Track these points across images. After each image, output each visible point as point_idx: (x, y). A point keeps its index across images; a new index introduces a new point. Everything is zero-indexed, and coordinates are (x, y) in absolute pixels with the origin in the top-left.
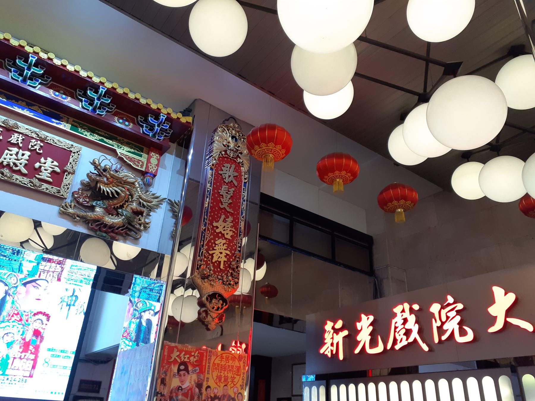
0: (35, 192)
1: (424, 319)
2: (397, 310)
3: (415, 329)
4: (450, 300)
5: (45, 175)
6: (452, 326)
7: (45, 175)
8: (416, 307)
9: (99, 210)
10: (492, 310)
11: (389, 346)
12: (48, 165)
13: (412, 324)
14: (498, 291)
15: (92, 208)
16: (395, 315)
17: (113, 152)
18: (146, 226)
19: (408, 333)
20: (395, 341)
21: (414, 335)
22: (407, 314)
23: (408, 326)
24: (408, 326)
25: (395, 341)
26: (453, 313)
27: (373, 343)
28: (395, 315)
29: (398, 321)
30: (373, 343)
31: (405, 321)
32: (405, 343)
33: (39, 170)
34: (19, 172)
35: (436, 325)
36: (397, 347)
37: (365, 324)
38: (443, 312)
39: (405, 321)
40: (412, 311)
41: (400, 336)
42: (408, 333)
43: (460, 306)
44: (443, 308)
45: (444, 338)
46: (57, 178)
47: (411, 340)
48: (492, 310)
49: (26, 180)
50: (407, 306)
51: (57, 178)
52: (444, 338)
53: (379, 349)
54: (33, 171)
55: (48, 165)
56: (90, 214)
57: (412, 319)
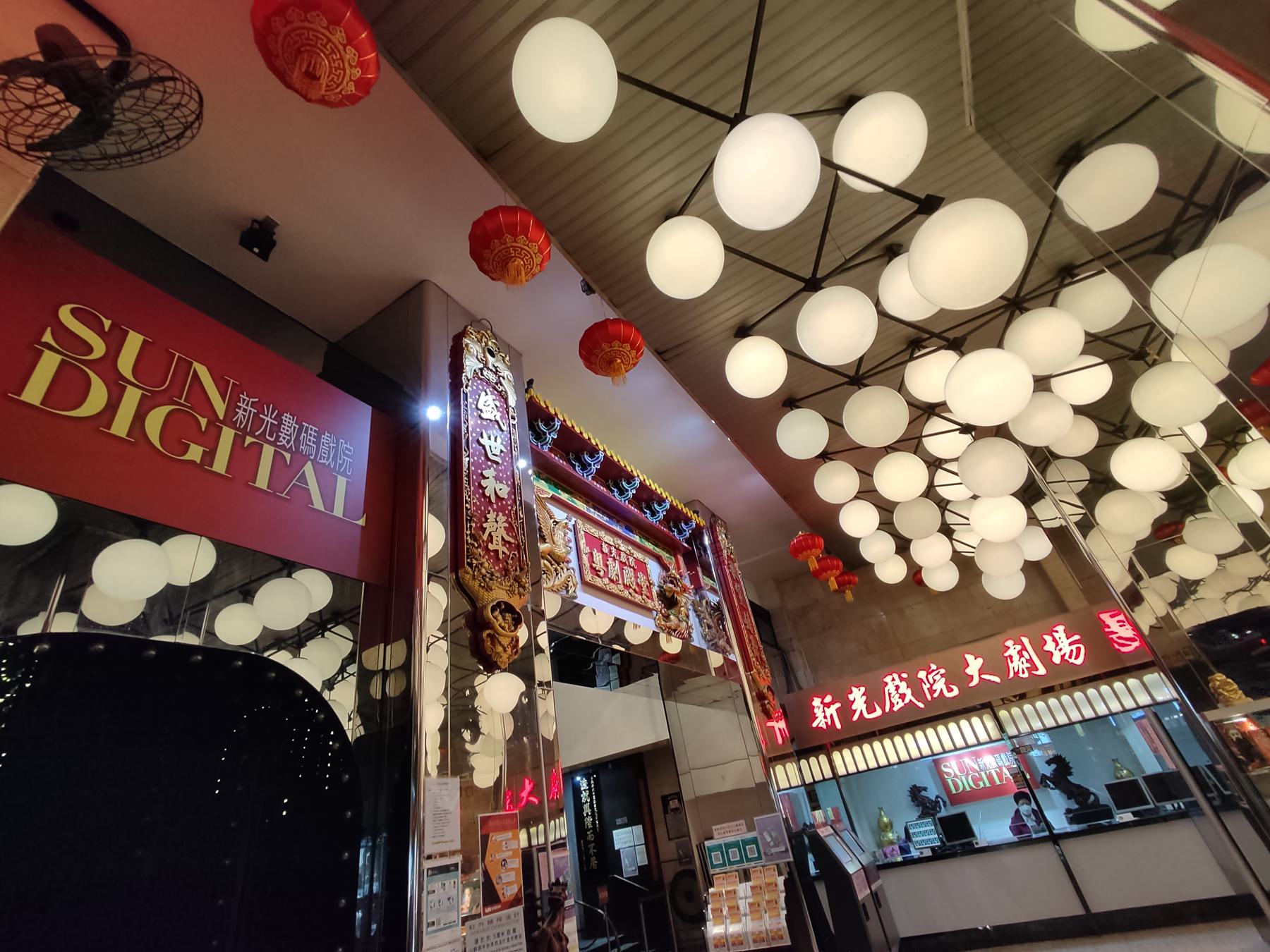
1: (915, 685)
2: (888, 679)
3: (908, 692)
4: (933, 667)
8: (904, 675)
11: (887, 709)
13: (903, 688)
20: (892, 705)
21: (909, 697)
22: (897, 682)
25: (892, 705)
27: (871, 709)
29: (890, 688)
30: (871, 709)
31: (897, 687)
32: (901, 704)
36: (896, 708)
37: (858, 698)
38: (930, 677)
39: (897, 687)
40: (902, 679)
41: (896, 699)
42: (903, 696)
44: (928, 673)
47: (907, 701)
50: (895, 676)
53: (879, 712)
57: (903, 685)
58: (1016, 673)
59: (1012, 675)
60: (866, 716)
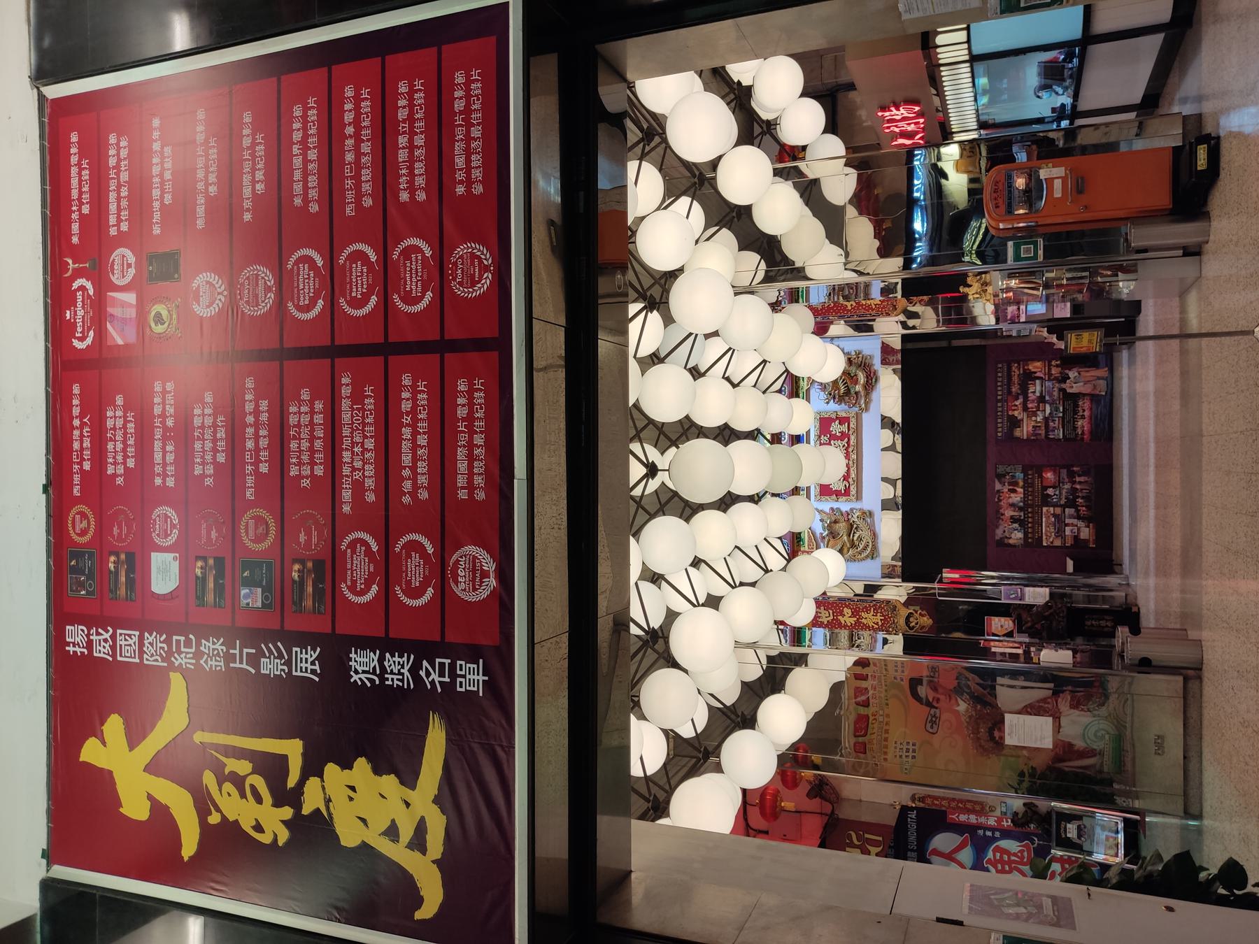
0: (858, 431)
5: (844, 428)
7: (844, 428)
9: (858, 388)
12: (836, 428)
15: (856, 393)
17: (808, 390)
18: (858, 353)
33: (842, 433)
34: (848, 443)
46: (843, 420)
49: (852, 438)
51: (843, 420)
54: (844, 436)
55: (836, 428)
56: (862, 393)
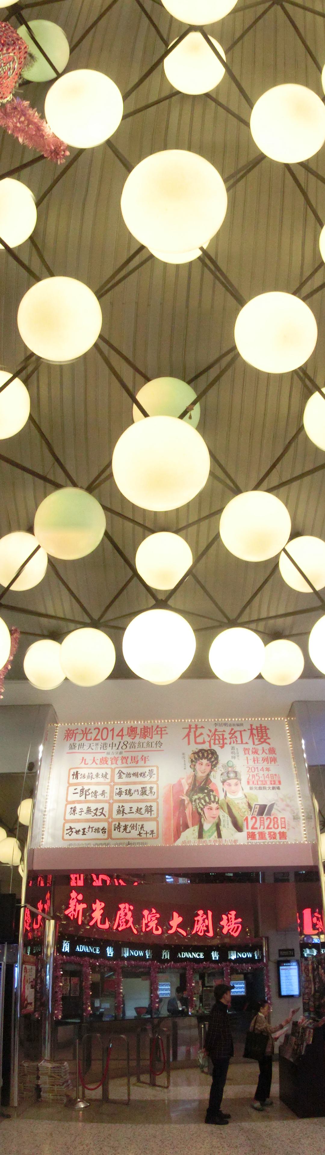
2: (122, 906)
3: (131, 920)
6: (153, 924)
10: (171, 923)
14: (175, 915)
16: (120, 909)
19: (127, 922)
20: (119, 925)
21: (130, 924)
22: (127, 910)
23: (127, 918)
24: (127, 918)
26: (154, 919)
27: (103, 922)
28: (120, 909)
29: (120, 913)
30: (103, 922)
31: (126, 915)
32: (124, 927)
35: (144, 922)
36: (120, 929)
43: (158, 916)
45: (147, 930)
47: (128, 926)
48: (171, 923)
52: (147, 930)
57: (130, 914)
58: (197, 932)
59: (194, 932)
60: (100, 926)
